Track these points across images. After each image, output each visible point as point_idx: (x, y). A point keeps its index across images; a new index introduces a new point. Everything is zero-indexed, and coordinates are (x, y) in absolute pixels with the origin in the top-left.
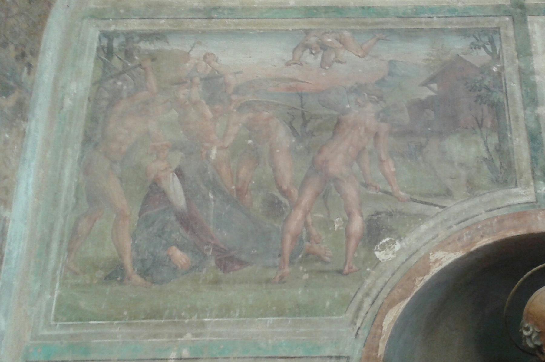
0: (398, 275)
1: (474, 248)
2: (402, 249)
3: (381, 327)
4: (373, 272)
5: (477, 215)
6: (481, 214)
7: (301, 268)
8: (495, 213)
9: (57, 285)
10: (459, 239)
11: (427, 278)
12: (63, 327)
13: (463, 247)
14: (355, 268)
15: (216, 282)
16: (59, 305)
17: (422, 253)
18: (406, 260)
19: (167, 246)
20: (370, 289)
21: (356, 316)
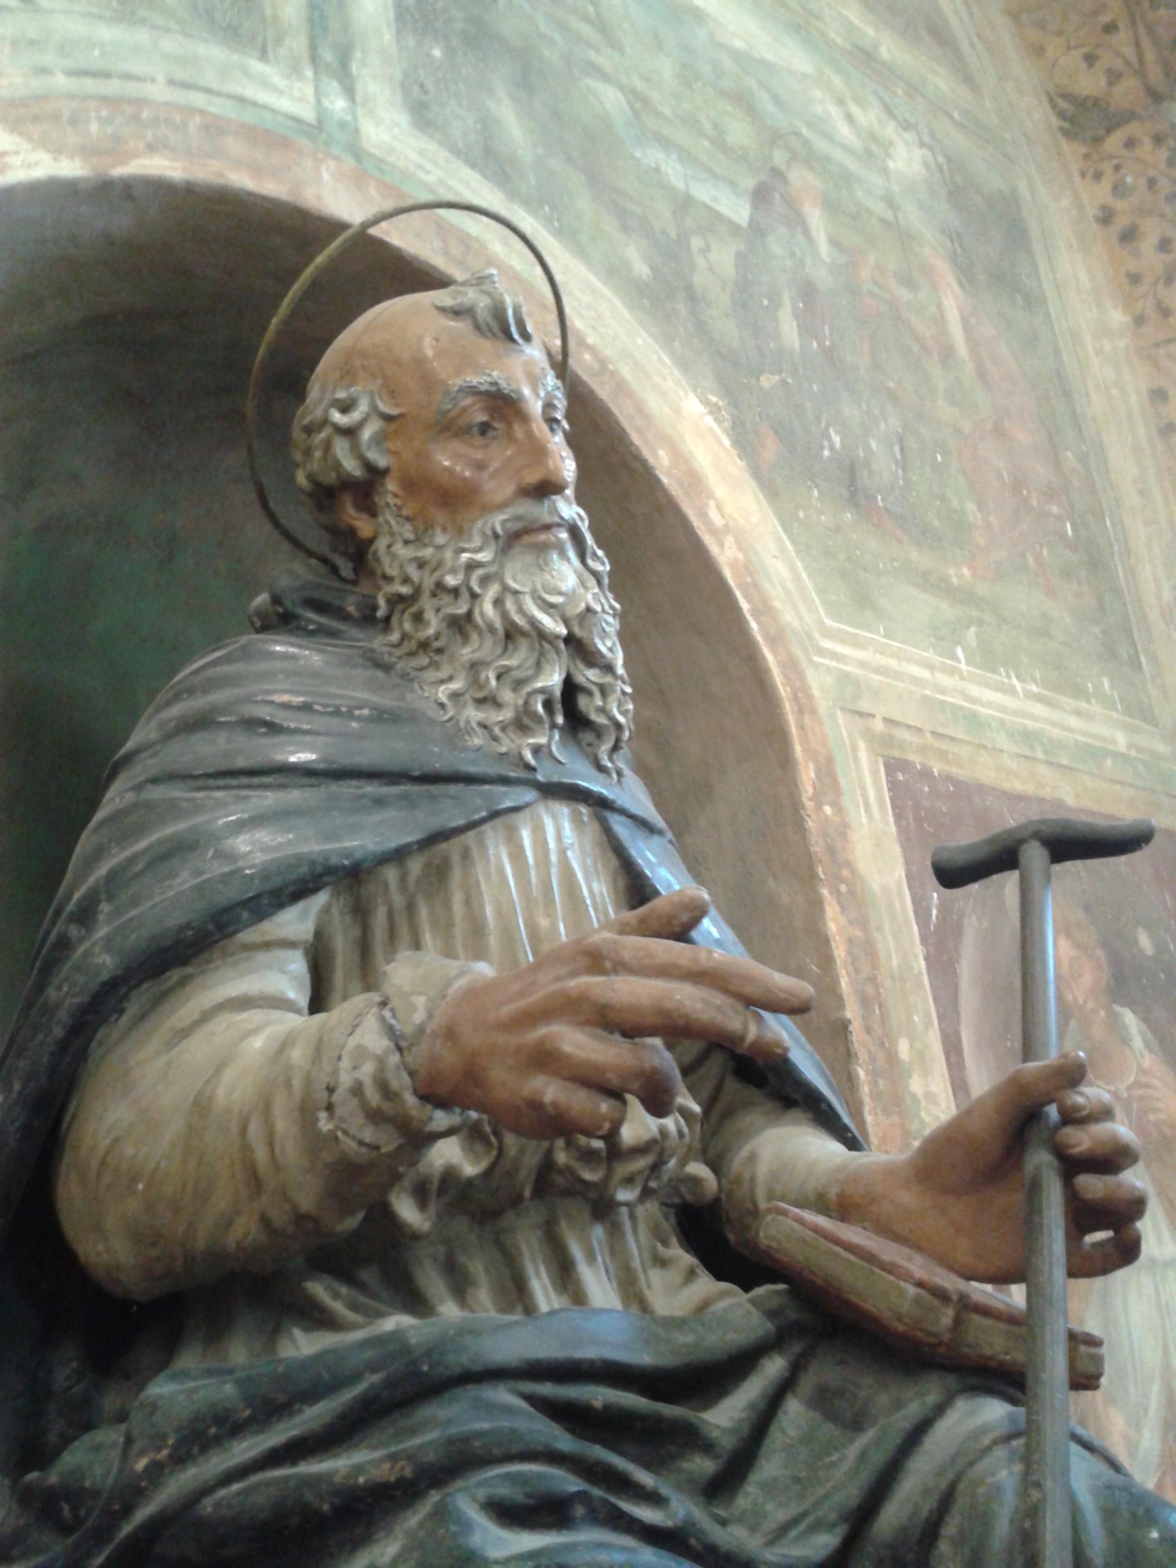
1: (119, 171)
5: (139, 79)
6: (153, 80)
8: (197, 99)
10: (74, 121)
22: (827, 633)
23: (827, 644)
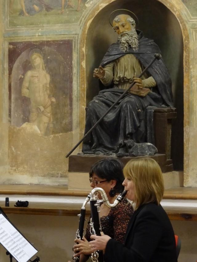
0: (91, 11)
2: (92, 3)
3: (86, 26)
4: (85, 11)
7: (67, 10)
9: (8, 17)
11: (98, 11)
12: (11, 28)
13: (108, 2)
14: (80, 9)
15: (46, 14)
16: (9, 22)
17: (97, 4)
18: (94, 6)
19: (33, 5)
20: (84, 15)
21: (80, 23)
22: (191, 19)
23: (191, 20)
